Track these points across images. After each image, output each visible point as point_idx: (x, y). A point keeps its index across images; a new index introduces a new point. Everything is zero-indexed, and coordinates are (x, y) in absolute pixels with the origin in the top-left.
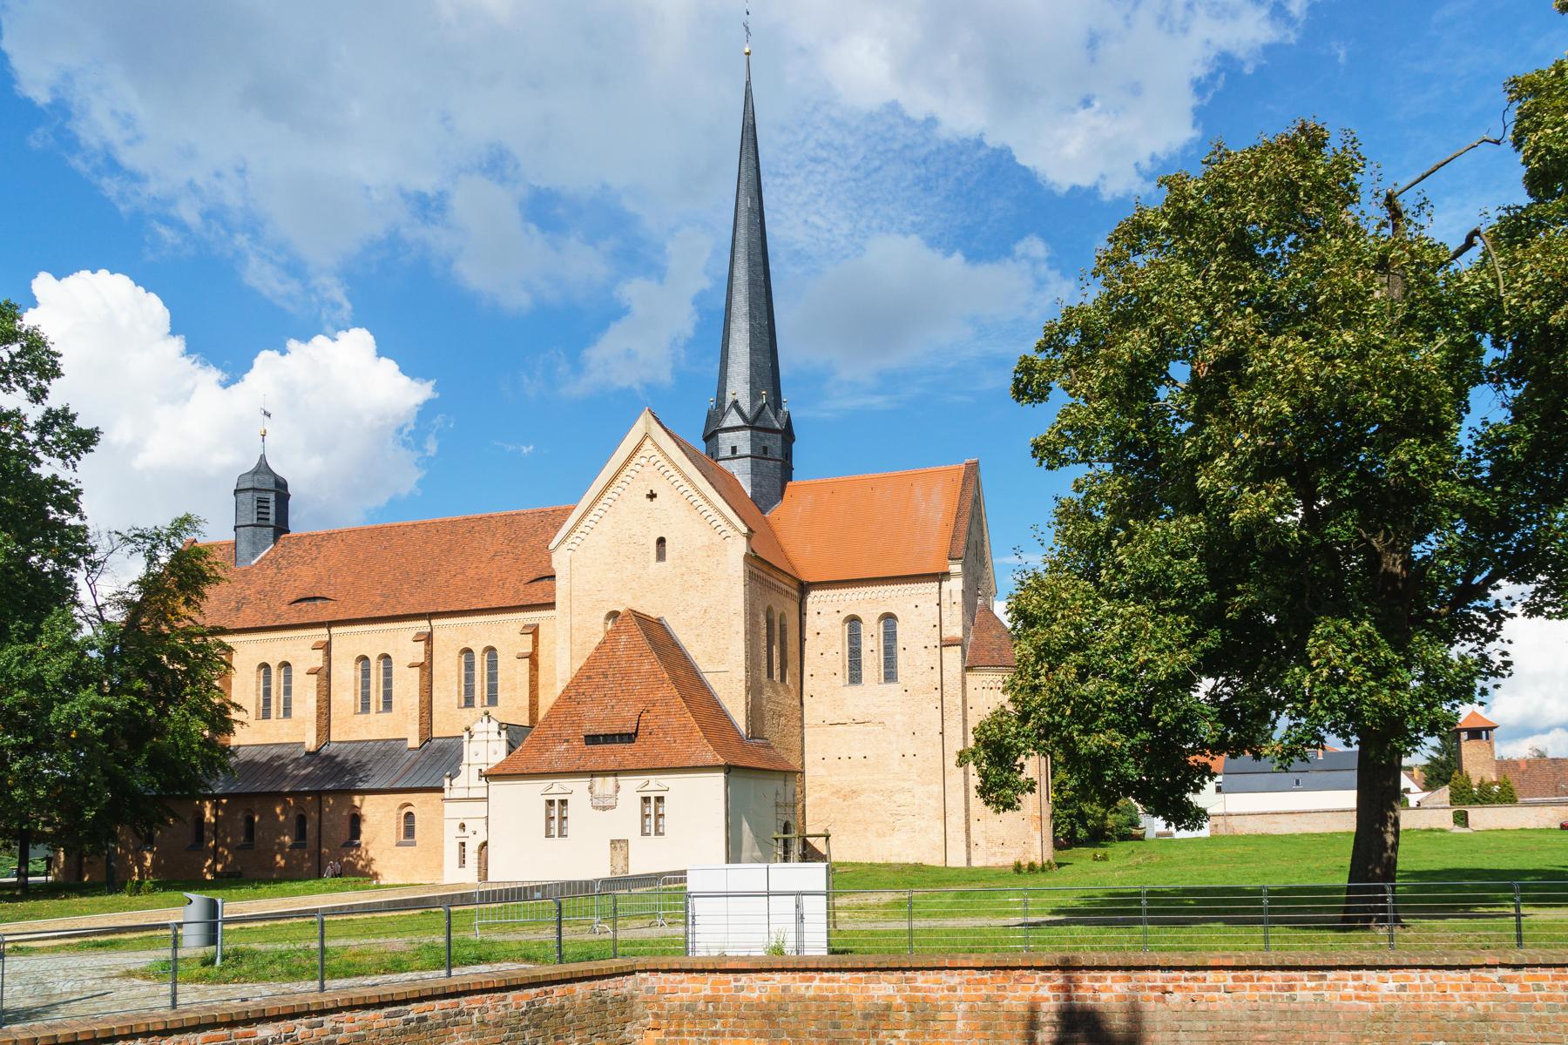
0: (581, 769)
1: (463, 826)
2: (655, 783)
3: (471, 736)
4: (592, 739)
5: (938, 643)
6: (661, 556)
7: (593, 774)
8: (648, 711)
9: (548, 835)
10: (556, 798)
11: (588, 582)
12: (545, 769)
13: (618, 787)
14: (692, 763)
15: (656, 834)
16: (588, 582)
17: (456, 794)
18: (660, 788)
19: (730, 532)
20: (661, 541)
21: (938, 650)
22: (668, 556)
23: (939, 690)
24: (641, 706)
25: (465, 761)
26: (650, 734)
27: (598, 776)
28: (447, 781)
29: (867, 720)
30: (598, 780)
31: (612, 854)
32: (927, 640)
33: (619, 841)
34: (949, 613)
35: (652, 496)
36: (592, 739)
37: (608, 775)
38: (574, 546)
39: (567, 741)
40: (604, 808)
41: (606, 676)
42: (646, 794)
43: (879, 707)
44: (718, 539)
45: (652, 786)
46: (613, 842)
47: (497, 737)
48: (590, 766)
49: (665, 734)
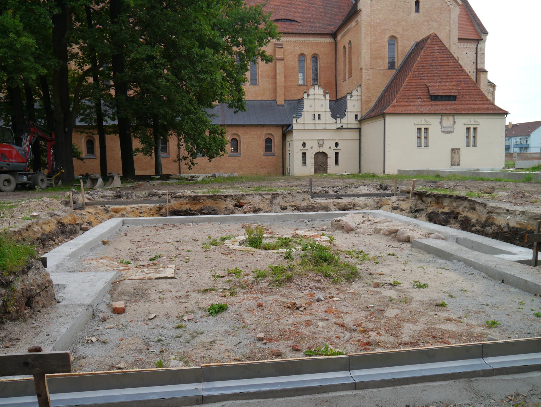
0: (437, 112)
1: (304, 145)
2: (470, 121)
3: (308, 95)
5: (475, 70)
6: (417, 10)
7: (442, 114)
8: (458, 85)
9: (419, 146)
10: (423, 127)
11: (379, 19)
12: (417, 112)
13: (454, 122)
16: (379, 19)
17: (301, 127)
22: (421, 10)
25: (305, 109)
26: (462, 97)
27: (444, 116)
28: (294, 121)
30: (445, 118)
31: (452, 156)
37: (450, 116)
39: (420, 98)
40: (448, 133)
41: (432, 66)
44: (445, 5)
45: (472, 123)
47: (324, 98)
48: (440, 111)
49: (470, 97)
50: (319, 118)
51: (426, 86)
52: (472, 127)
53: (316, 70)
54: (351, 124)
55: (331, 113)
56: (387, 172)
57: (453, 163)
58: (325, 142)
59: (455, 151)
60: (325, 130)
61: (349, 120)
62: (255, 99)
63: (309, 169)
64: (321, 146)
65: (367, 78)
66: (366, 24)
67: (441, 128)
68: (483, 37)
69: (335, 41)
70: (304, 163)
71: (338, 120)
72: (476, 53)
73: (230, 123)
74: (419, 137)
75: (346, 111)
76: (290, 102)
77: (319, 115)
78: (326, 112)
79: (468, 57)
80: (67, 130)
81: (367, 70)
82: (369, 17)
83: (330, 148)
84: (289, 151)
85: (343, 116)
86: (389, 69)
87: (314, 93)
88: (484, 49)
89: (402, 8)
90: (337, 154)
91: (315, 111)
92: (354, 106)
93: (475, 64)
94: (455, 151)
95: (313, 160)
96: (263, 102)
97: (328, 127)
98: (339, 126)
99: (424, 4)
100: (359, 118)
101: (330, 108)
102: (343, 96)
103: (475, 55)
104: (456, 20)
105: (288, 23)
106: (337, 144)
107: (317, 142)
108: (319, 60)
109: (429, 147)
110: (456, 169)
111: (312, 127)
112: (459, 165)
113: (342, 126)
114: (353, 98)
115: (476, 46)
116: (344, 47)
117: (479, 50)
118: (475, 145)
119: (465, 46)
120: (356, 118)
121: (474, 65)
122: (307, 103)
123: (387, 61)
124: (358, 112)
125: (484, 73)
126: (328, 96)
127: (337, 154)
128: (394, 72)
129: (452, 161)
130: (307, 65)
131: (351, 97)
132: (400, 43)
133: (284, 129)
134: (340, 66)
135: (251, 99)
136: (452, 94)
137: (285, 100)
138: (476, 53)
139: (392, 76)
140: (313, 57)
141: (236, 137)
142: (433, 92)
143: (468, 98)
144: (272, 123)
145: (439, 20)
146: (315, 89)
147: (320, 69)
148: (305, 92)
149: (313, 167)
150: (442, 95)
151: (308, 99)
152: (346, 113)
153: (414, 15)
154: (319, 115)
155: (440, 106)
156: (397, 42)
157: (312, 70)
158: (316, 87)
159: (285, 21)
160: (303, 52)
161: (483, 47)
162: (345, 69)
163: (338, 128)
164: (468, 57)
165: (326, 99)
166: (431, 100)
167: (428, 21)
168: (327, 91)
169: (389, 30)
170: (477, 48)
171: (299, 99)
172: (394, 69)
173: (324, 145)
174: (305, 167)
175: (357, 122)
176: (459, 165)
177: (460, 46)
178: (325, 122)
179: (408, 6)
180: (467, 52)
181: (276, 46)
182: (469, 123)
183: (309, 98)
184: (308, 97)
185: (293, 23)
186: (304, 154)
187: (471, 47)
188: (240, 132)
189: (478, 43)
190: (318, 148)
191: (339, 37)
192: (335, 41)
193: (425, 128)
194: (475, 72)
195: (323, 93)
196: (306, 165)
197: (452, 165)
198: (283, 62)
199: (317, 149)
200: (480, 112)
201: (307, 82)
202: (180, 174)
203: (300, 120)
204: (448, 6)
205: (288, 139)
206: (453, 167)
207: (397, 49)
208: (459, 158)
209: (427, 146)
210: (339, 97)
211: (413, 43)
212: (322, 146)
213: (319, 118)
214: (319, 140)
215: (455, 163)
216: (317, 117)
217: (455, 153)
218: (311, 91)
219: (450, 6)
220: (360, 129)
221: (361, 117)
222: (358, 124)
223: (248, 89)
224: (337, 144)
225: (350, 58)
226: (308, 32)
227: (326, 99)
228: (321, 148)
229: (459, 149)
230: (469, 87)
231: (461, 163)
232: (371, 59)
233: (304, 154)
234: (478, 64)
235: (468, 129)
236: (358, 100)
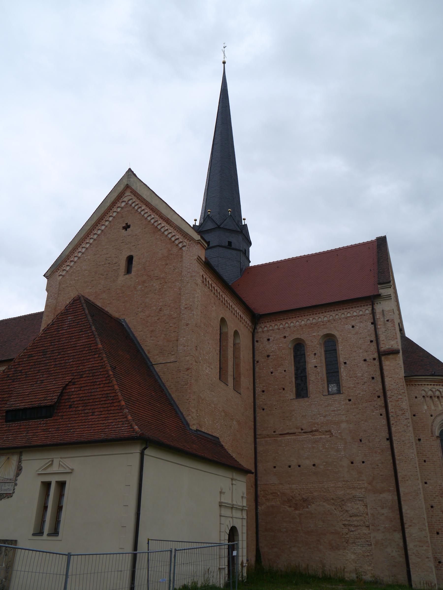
5: (376, 355)
6: (128, 270)
13: (19, 469)
14: (103, 436)
19: (186, 242)
20: (130, 259)
21: (377, 362)
22: (134, 269)
23: (382, 398)
24: (68, 378)
26: (70, 407)
29: (314, 429)
34: (384, 330)
35: (127, 227)
42: (46, 479)
43: (325, 417)
44: (175, 250)
45: (55, 468)
52: (54, 480)
68: (384, 292)
72: (374, 323)
79: (357, 333)
93: (374, 343)
109: (59, 537)
115: (370, 309)
117: (378, 316)
119: (349, 315)
121: (373, 347)
153: (122, 279)
164: (357, 333)
167: (144, 282)
179: (114, 268)
180: (353, 323)
187: (361, 313)
189: (373, 305)
194: (377, 359)
219: (184, 249)
234: (382, 342)
235: (47, 485)
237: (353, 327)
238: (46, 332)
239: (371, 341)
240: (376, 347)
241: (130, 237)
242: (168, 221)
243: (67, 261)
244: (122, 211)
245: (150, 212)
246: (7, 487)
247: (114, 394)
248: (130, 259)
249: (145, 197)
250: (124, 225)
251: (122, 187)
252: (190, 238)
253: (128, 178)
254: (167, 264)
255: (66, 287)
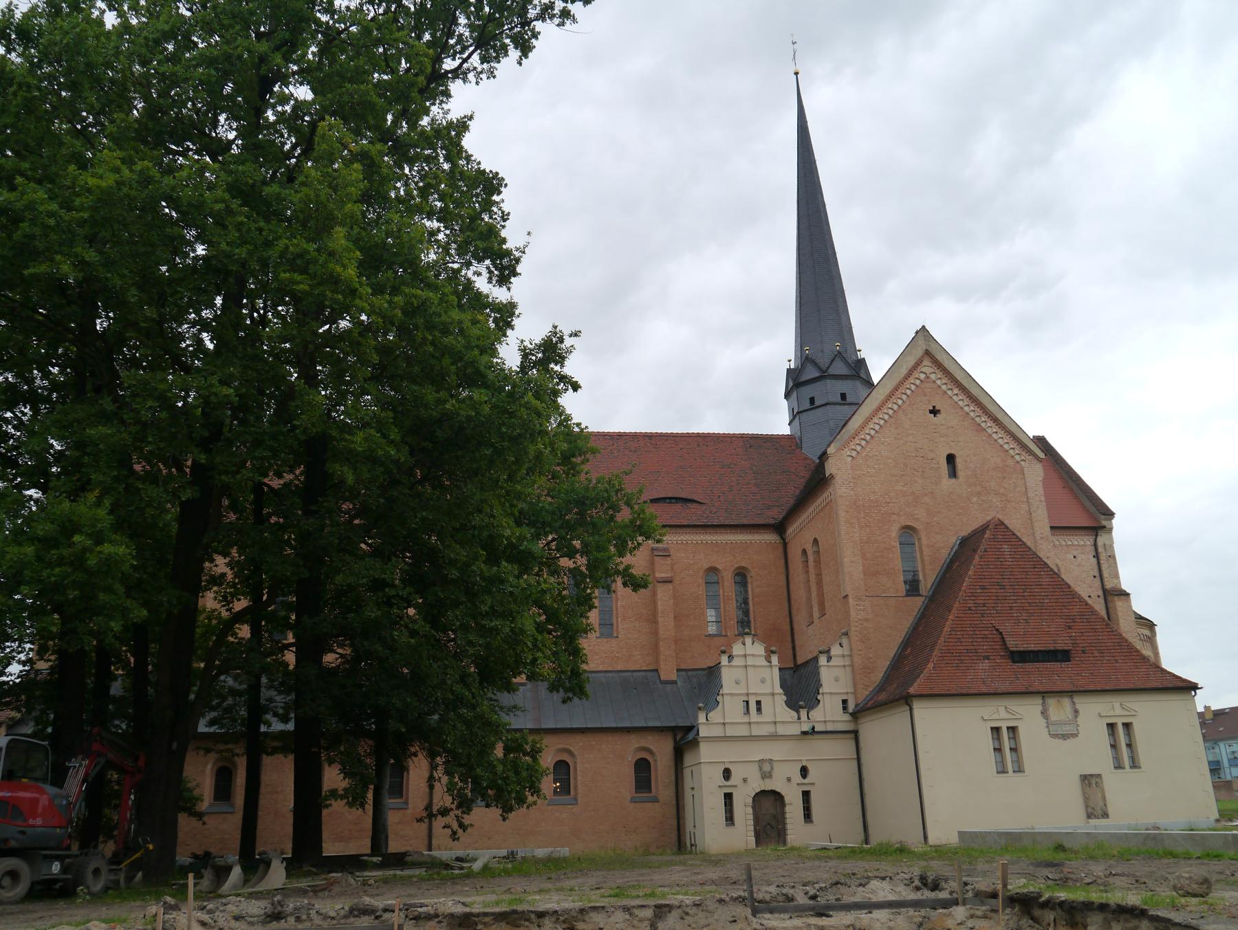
0: (1031, 689)
1: (727, 774)
3: (731, 657)
4: (1021, 657)
5: (1100, 593)
6: (953, 473)
7: (1044, 694)
8: (1070, 627)
9: (1002, 771)
10: (1004, 726)
12: (984, 689)
13: (1076, 712)
15: (1131, 767)
17: (717, 731)
18: (1126, 713)
19: (1025, 455)
20: (951, 459)
25: (725, 690)
26: (1084, 652)
27: (1050, 697)
28: (702, 718)
30: (1052, 702)
31: (1084, 793)
32: (1090, 590)
33: (1091, 776)
35: (934, 412)
36: (1021, 657)
38: (854, 454)
39: (987, 658)
40: (1064, 737)
41: (1003, 587)
45: (1118, 711)
46: (1085, 778)
47: (766, 663)
48: (1037, 686)
50: (759, 710)
51: (997, 630)
53: (746, 602)
54: (833, 721)
55: (784, 698)
56: (932, 840)
57: (1090, 811)
58: (775, 765)
59: (1089, 781)
60: (774, 737)
61: (829, 712)
62: (610, 669)
63: (743, 834)
64: (766, 776)
65: (860, 617)
66: (847, 503)
67: (1048, 727)
68: (1104, 523)
69: (784, 539)
70: (730, 819)
71: (803, 713)
72: (1097, 556)
73: (552, 725)
74: (998, 750)
75: (821, 691)
76: (690, 673)
77: (759, 703)
78: (773, 694)
79: (1079, 565)
80: (175, 746)
81: (859, 599)
82: (852, 490)
83: (789, 780)
84: (693, 789)
85: (813, 703)
86: (907, 595)
87: (743, 653)
88: (1111, 546)
89: (920, 470)
90: (806, 795)
91: (748, 694)
92: (837, 680)
93: (1098, 579)
94: (1086, 779)
95: (750, 810)
96: (629, 674)
97: (781, 730)
98: (806, 728)
99: (966, 462)
100: (851, 707)
101: (782, 687)
102: (809, 658)
103: (1094, 561)
104: (1041, 490)
105: (678, 507)
106: (804, 771)
107: (755, 767)
108: (749, 580)
110: (1099, 826)
111: (743, 731)
112: (1105, 815)
113: (813, 728)
114: (833, 662)
115: (1092, 540)
116: (804, 552)
117: (1100, 550)
118: (1135, 765)
120: (845, 708)
121: (1097, 582)
122: (729, 677)
123: (902, 578)
124: (847, 693)
125: (1123, 597)
126: (775, 659)
127: (806, 795)
128: (919, 602)
129: (1087, 807)
130: (724, 592)
131: (829, 659)
132: (924, 540)
133: (678, 738)
134: (799, 593)
135: (601, 668)
136: (1060, 647)
137: (678, 670)
138: (1097, 556)
139: (917, 610)
140: (737, 574)
141: (565, 757)
142: (1013, 644)
143: (1097, 654)
144: (651, 724)
145: (1002, 491)
146: (744, 644)
147: (753, 599)
148: (723, 652)
149: (752, 828)
150: (1036, 649)
151: (730, 666)
152: (819, 697)
153: (947, 483)
154: (759, 703)
155: (1037, 674)
156: (919, 539)
157: (737, 601)
158: (748, 640)
159: (673, 501)
160: (714, 565)
161: (1107, 543)
162: (809, 599)
163: (804, 733)
164: (1079, 565)
165: (771, 667)
166: (1014, 662)
167: (979, 494)
168: (773, 648)
169: (898, 514)
170: (1095, 545)
171: (711, 668)
172: (920, 595)
173: (774, 774)
174: (731, 829)
175: (847, 717)
176: (1105, 815)
177: (1058, 543)
178: (771, 719)
180: (1075, 553)
181: (656, 553)
182: (1111, 713)
183: (733, 663)
184: (729, 662)
185: (689, 505)
186: (728, 797)
187: (1082, 543)
188: (576, 744)
189: (1097, 536)
190: (761, 782)
191: (790, 531)
192: (784, 539)
193: (1008, 728)
194: (1102, 597)
195: (763, 653)
196: (733, 824)
197: (1089, 816)
198: (670, 586)
199: (757, 785)
200: (1131, 686)
201: (726, 628)
202: (430, 849)
203: (715, 716)
204: (1018, 462)
205: (688, 760)
206: (1093, 822)
207: (921, 553)
208: (1104, 798)
209: (1019, 769)
210: (800, 661)
211: (954, 540)
212: (770, 777)
213: (759, 710)
214: (761, 761)
215: (1096, 811)
216: (753, 706)
217: (1090, 784)
218: (737, 649)
219: (1022, 463)
220: (855, 734)
221: (856, 705)
222: (850, 721)
223: (595, 645)
224: (804, 771)
225: (819, 575)
226: (722, 523)
227: (771, 667)
228: (767, 780)
229: (1099, 776)
230: (1095, 630)
231: (1110, 811)
232: (864, 575)
233: (728, 797)
234: (1106, 580)
236: (844, 666)
237: (1075, 557)
238: (983, 560)
239: (1095, 577)
240: (1099, 583)
241: (944, 427)
242: (996, 420)
243: (854, 438)
244: (923, 386)
245: (967, 401)
246: (1068, 728)
247: (1126, 644)
248: (951, 459)
249: (959, 378)
250: (932, 408)
251: (919, 352)
252: (1030, 452)
253: (925, 340)
254: (1005, 478)
255: (864, 475)
